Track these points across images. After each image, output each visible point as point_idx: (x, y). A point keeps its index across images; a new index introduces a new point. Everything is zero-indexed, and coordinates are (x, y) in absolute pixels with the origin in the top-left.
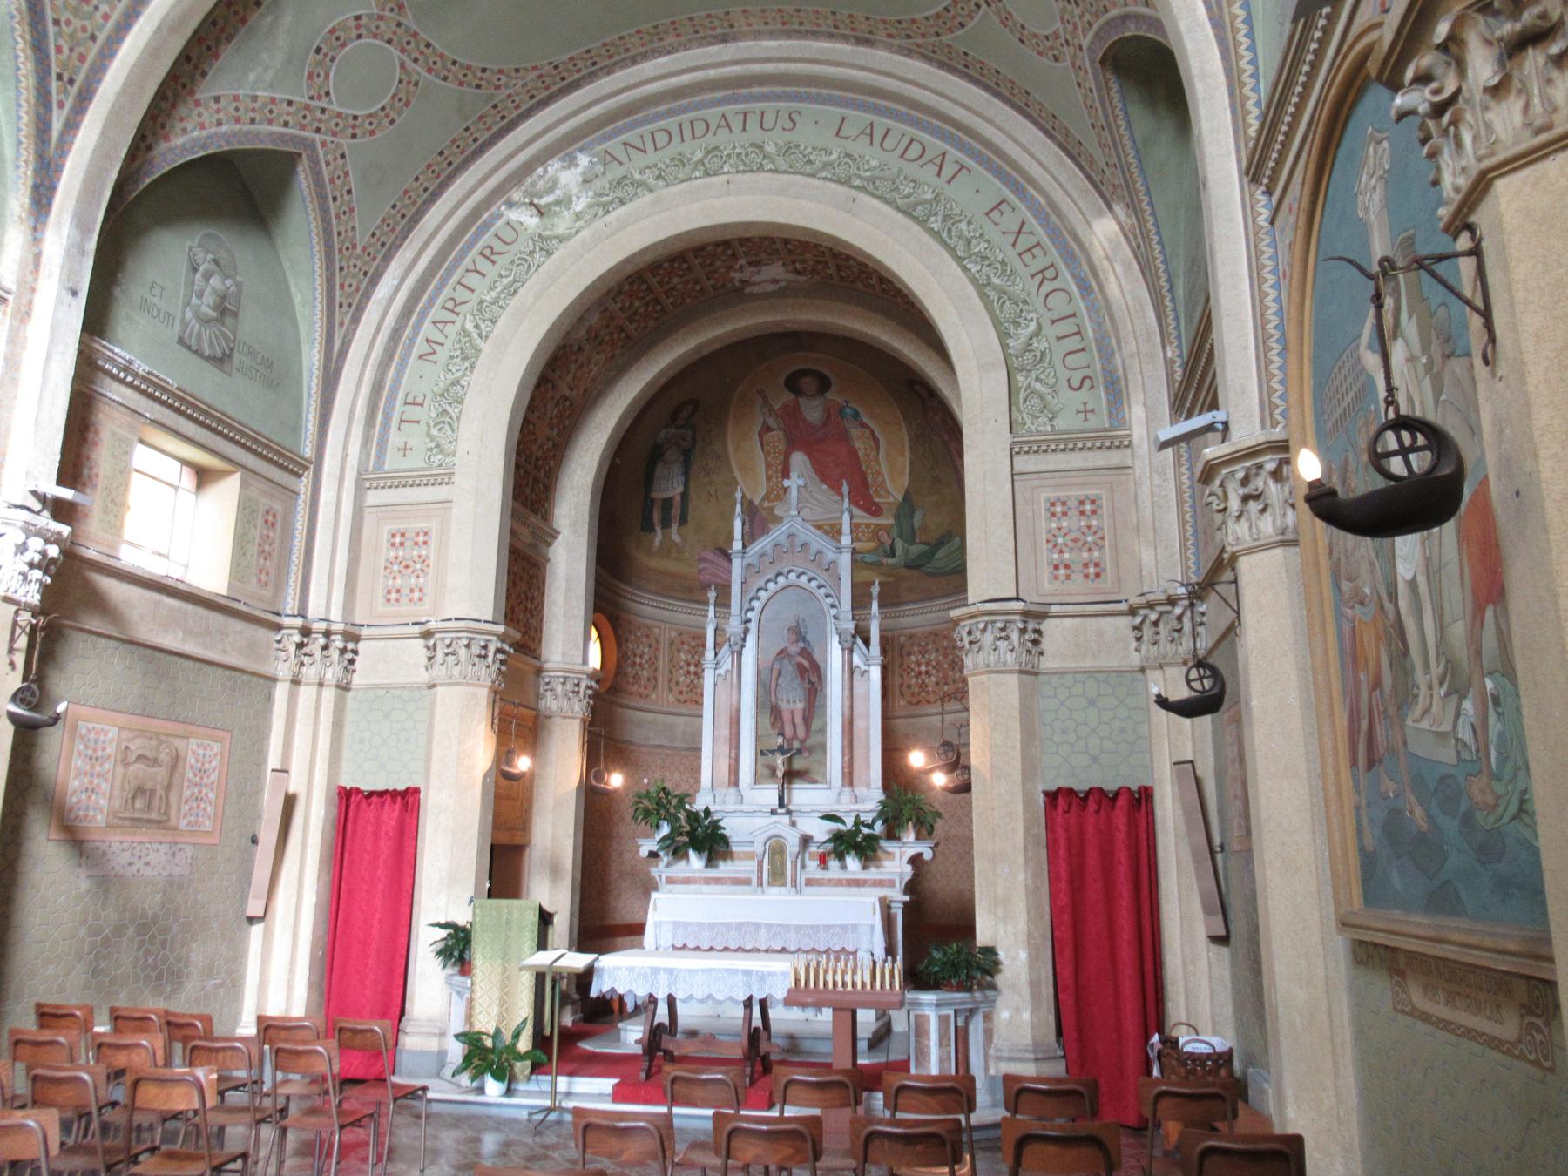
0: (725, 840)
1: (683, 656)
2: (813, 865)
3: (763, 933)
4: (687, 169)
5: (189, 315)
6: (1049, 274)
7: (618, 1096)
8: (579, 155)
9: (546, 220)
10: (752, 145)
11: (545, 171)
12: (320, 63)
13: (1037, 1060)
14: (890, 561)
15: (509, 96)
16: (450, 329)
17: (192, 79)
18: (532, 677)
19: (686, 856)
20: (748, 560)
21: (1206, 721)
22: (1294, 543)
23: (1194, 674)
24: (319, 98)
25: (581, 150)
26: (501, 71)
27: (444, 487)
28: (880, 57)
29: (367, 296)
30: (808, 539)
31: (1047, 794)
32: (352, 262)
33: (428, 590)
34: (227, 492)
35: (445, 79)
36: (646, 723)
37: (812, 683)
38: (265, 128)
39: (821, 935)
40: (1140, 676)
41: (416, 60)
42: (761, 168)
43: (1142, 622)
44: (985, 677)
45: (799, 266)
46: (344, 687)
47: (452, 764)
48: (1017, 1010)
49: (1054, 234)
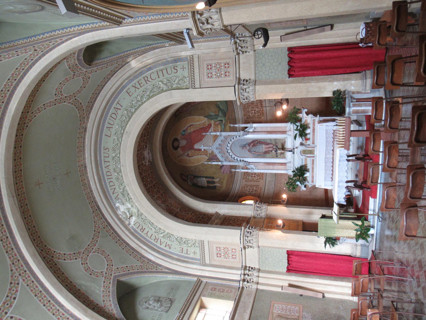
0: (301, 167)
1: (250, 178)
2: (308, 142)
3: (328, 156)
4: (119, 177)
5: (160, 310)
6: (146, 79)
7: (375, 197)
8: (116, 206)
9: (133, 215)
10: (113, 160)
11: (121, 215)
12: (94, 274)
13: (366, 79)
14: (224, 121)
15: (101, 224)
16: (162, 241)
17: (98, 307)
19: (306, 177)
20: (224, 161)
21: (270, 32)
22: (220, 9)
23: (257, 37)
24: (103, 274)
25: (115, 205)
26: (95, 226)
27: (205, 243)
28: (89, 125)
29: (154, 262)
30: (218, 144)
31: (289, 77)
32: (145, 266)
33: (232, 247)
34: (206, 300)
35: (97, 241)
36: (268, 188)
37: (258, 143)
38: (111, 289)
39: (329, 140)
40: (256, 52)
41: (93, 249)
42: (119, 157)
43: (241, 51)
44: (256, 95)
45: (145, 147)
46: (259, 270)
47: (281, 242)
48: (351, 84)
49: (136, 77)
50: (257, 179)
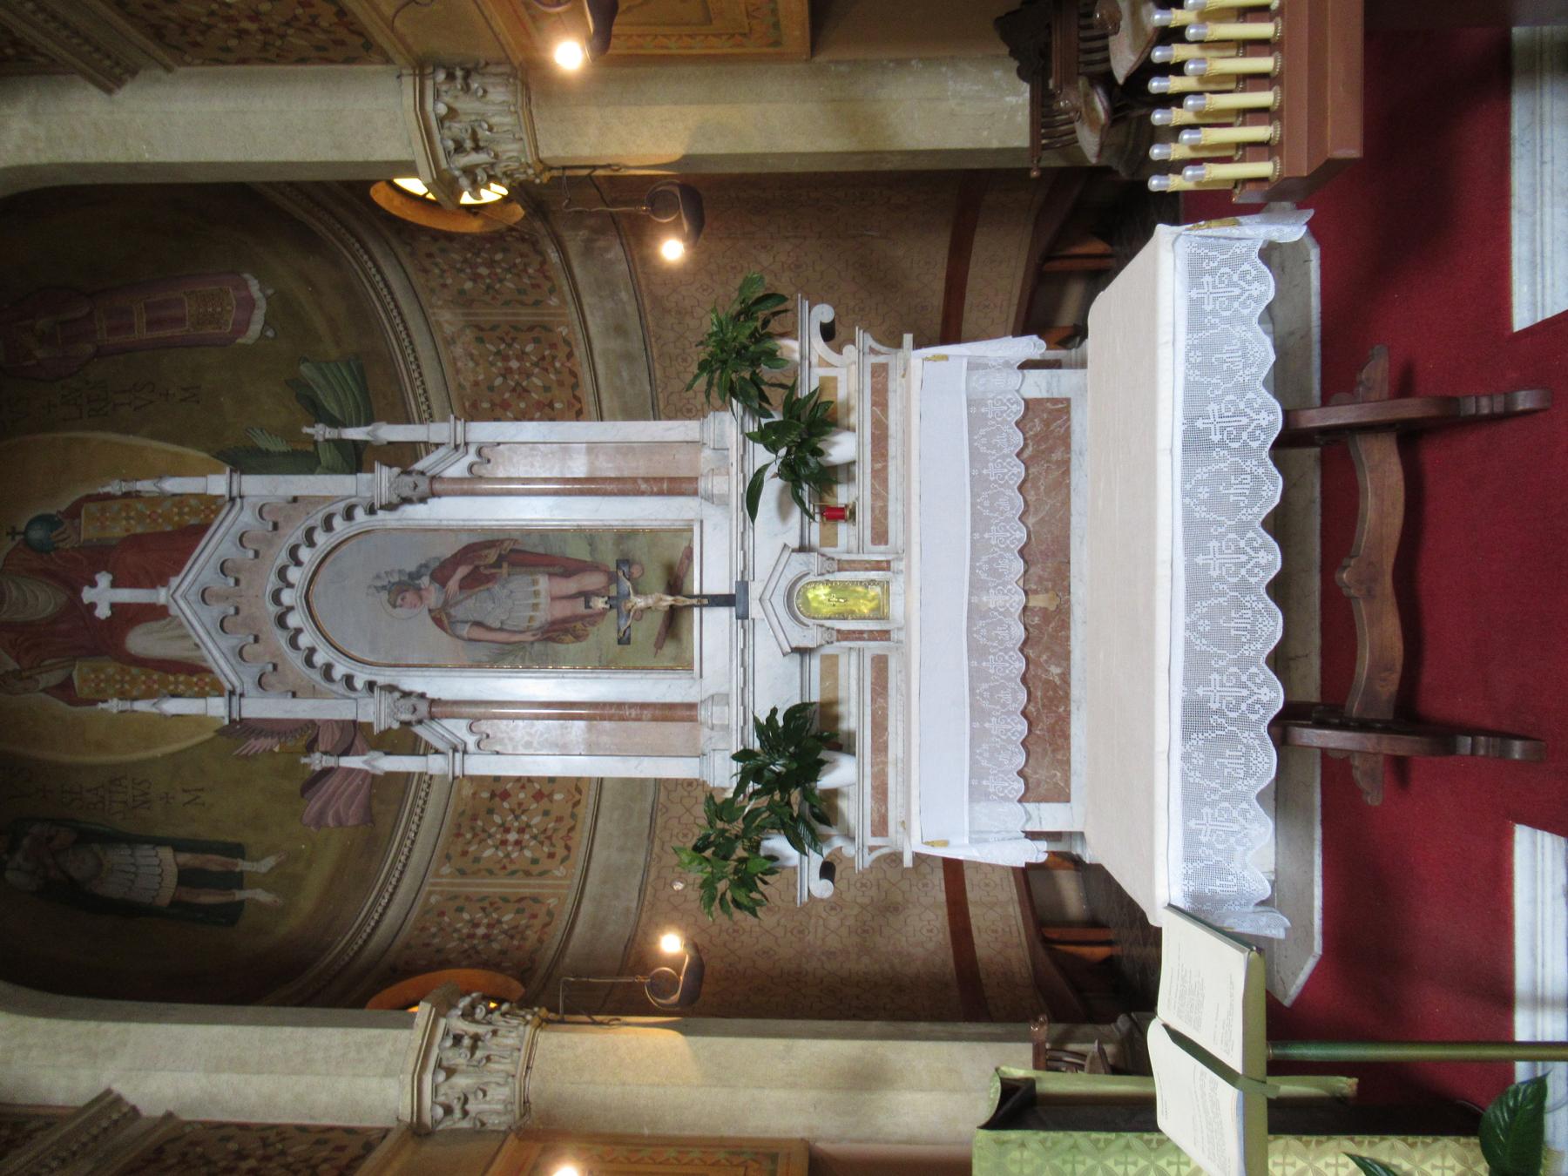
1: (488, 853)
3: (992, 600)
18: (428, 1149)
19: (833, 794)
20: (249, 686)
30: (214, 563)
39: (991, 471)
50: (535, 861)
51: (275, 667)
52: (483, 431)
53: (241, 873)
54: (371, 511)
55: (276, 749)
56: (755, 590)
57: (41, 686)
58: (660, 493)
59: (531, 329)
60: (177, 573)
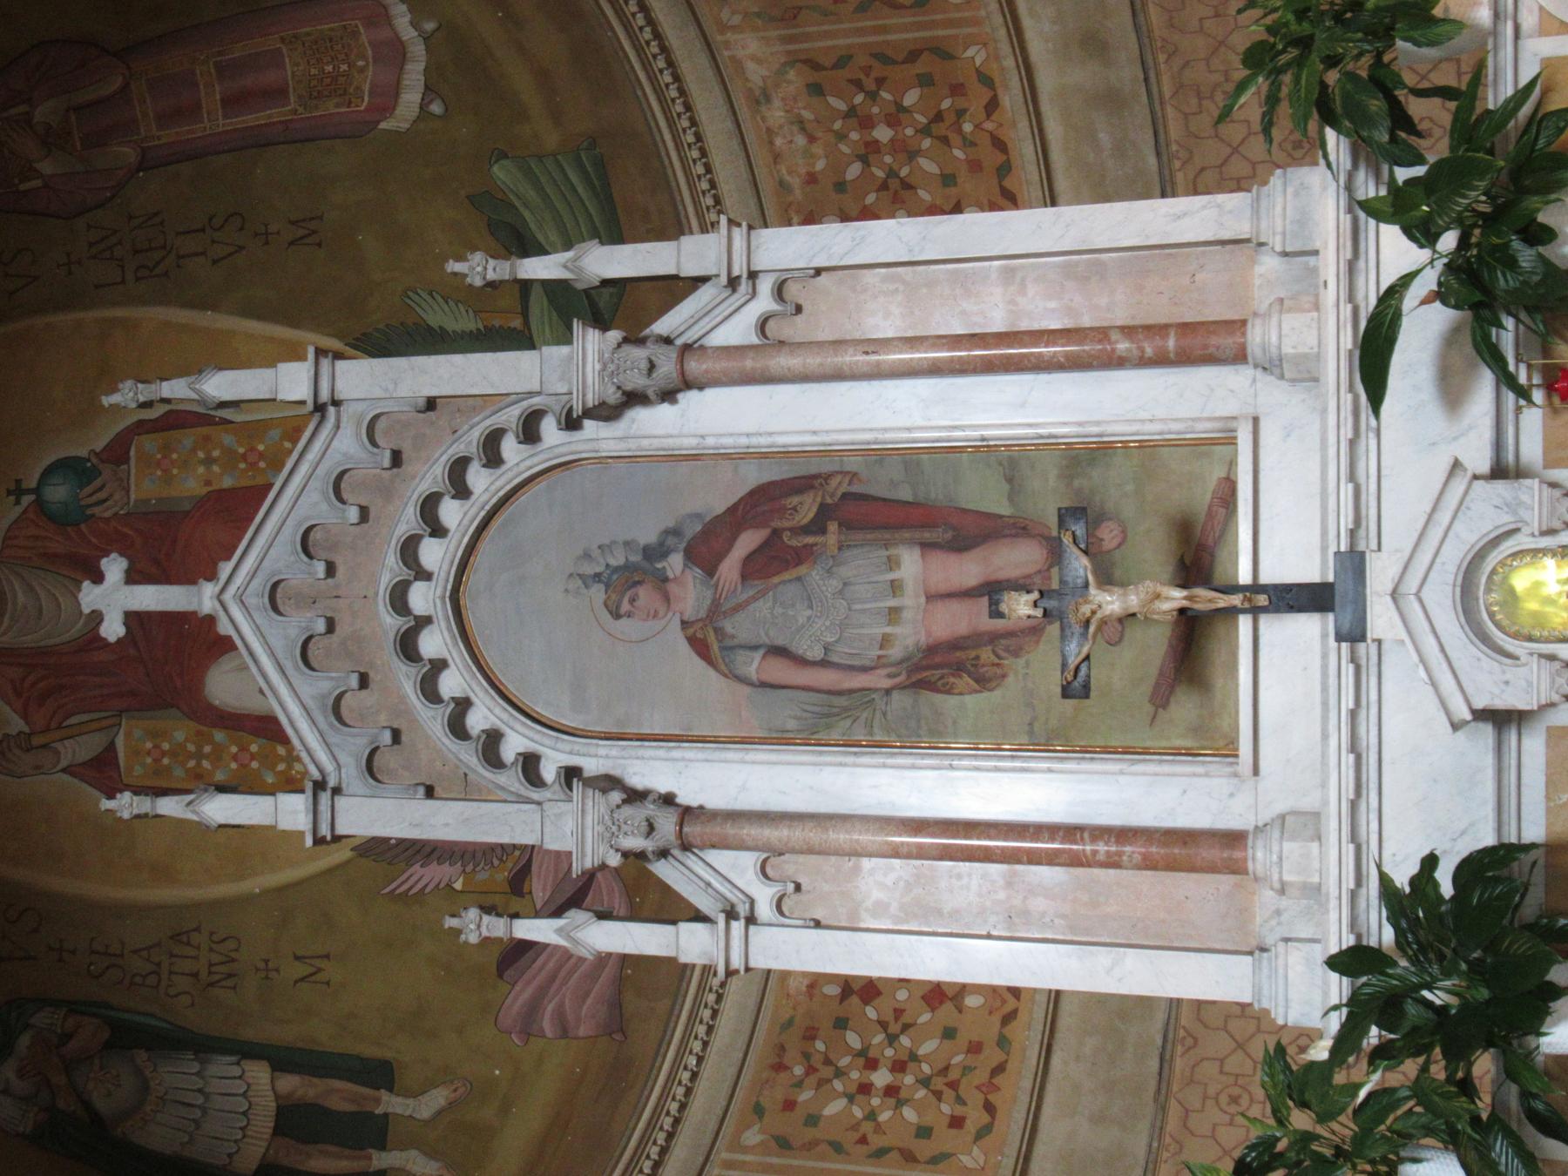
1: (834, 1107)
30: (292, 534)
50: (924, 1132)
51: (396, 736)
52: (786, 247)
53: (386, 1115)
54: (571, 423)
55: (458, 886)
56: (1381, 573)
57: (64, 763)
58: (1161, 360)
59: (913, 56)
60: (229, 558)
